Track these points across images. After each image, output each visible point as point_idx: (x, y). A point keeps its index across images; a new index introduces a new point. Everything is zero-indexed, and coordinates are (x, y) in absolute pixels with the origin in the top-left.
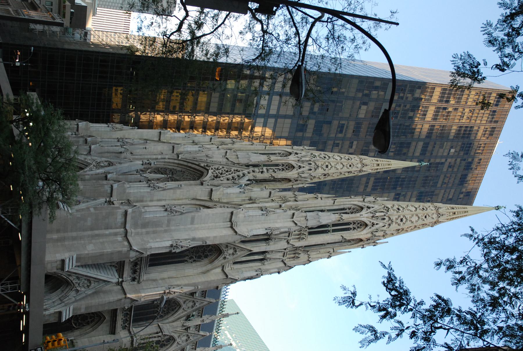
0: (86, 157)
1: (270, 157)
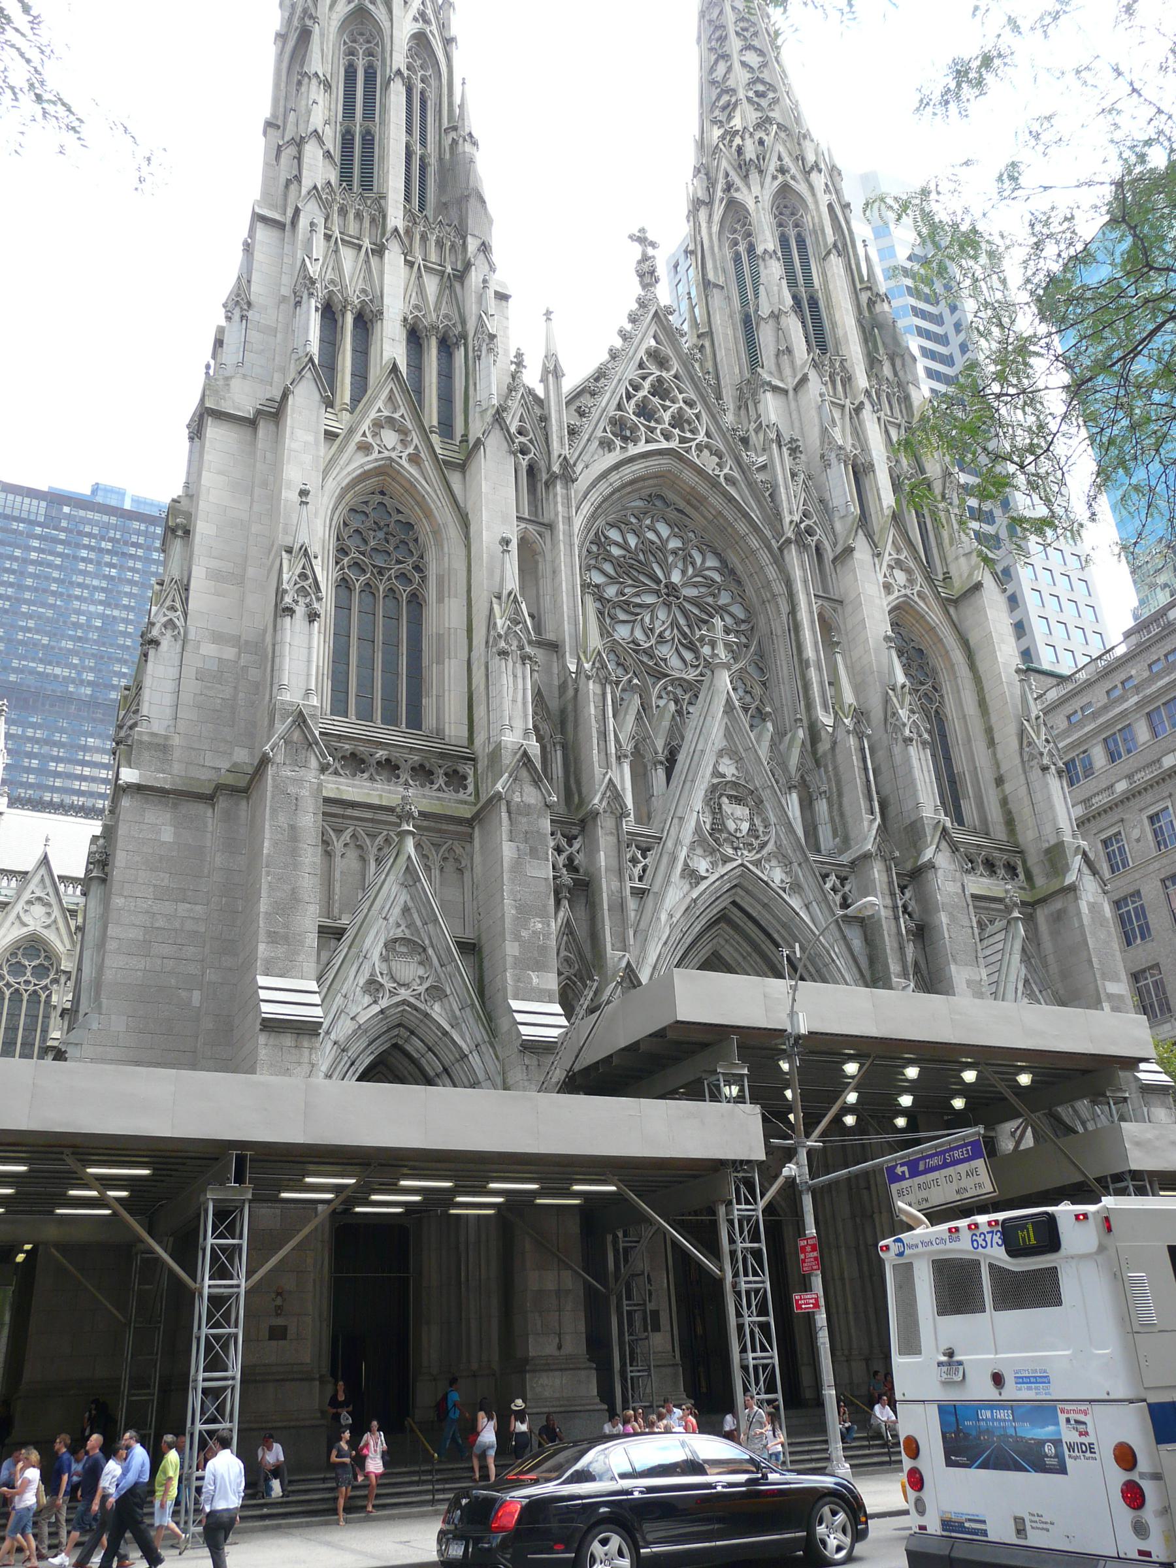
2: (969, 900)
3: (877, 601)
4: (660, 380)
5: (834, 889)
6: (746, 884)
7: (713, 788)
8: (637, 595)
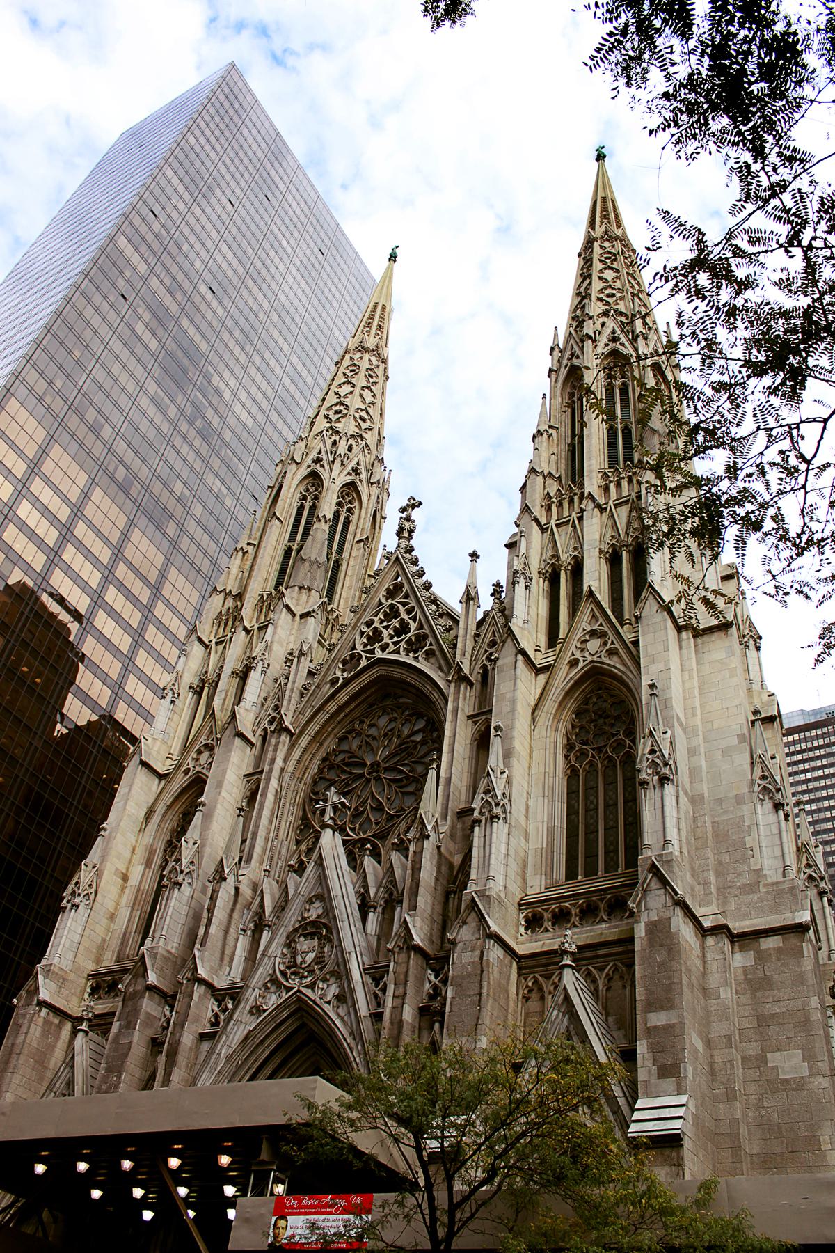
0: (246, 1006)
1: (325, 516)
4: (392, 606)
6: (303, 1006)
7: (296, 930)
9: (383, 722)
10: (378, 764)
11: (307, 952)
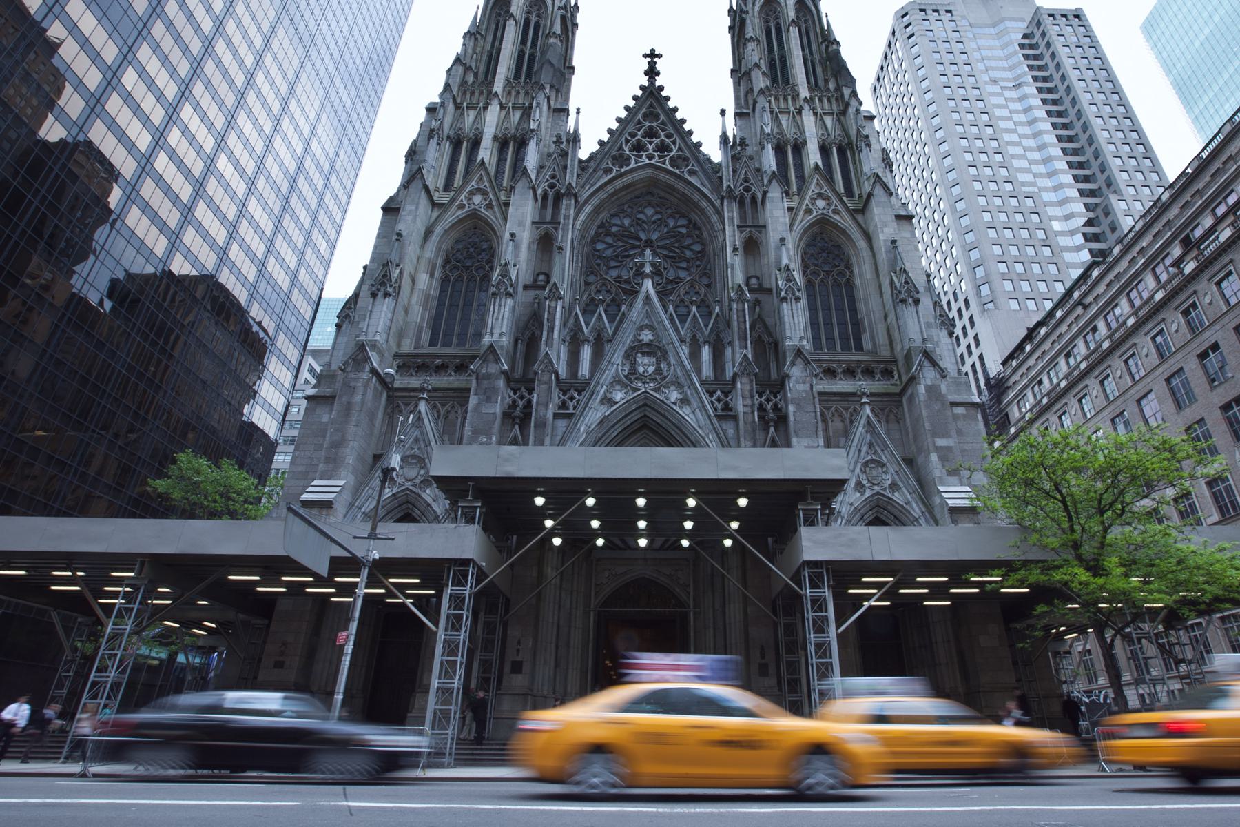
2: (816, 395)
3: (781, 219)
4: (651, 128)
5: (719, 400)
6: (649, 403)
7: (632, 348)
8: (626, 250)
9: (650, 211)
10: (652, 242)
11: (649, 365)
